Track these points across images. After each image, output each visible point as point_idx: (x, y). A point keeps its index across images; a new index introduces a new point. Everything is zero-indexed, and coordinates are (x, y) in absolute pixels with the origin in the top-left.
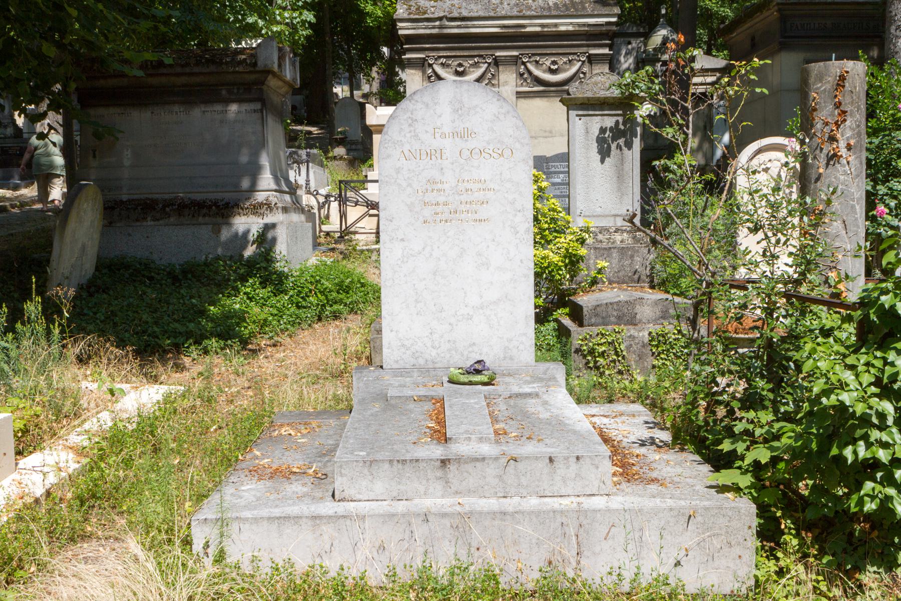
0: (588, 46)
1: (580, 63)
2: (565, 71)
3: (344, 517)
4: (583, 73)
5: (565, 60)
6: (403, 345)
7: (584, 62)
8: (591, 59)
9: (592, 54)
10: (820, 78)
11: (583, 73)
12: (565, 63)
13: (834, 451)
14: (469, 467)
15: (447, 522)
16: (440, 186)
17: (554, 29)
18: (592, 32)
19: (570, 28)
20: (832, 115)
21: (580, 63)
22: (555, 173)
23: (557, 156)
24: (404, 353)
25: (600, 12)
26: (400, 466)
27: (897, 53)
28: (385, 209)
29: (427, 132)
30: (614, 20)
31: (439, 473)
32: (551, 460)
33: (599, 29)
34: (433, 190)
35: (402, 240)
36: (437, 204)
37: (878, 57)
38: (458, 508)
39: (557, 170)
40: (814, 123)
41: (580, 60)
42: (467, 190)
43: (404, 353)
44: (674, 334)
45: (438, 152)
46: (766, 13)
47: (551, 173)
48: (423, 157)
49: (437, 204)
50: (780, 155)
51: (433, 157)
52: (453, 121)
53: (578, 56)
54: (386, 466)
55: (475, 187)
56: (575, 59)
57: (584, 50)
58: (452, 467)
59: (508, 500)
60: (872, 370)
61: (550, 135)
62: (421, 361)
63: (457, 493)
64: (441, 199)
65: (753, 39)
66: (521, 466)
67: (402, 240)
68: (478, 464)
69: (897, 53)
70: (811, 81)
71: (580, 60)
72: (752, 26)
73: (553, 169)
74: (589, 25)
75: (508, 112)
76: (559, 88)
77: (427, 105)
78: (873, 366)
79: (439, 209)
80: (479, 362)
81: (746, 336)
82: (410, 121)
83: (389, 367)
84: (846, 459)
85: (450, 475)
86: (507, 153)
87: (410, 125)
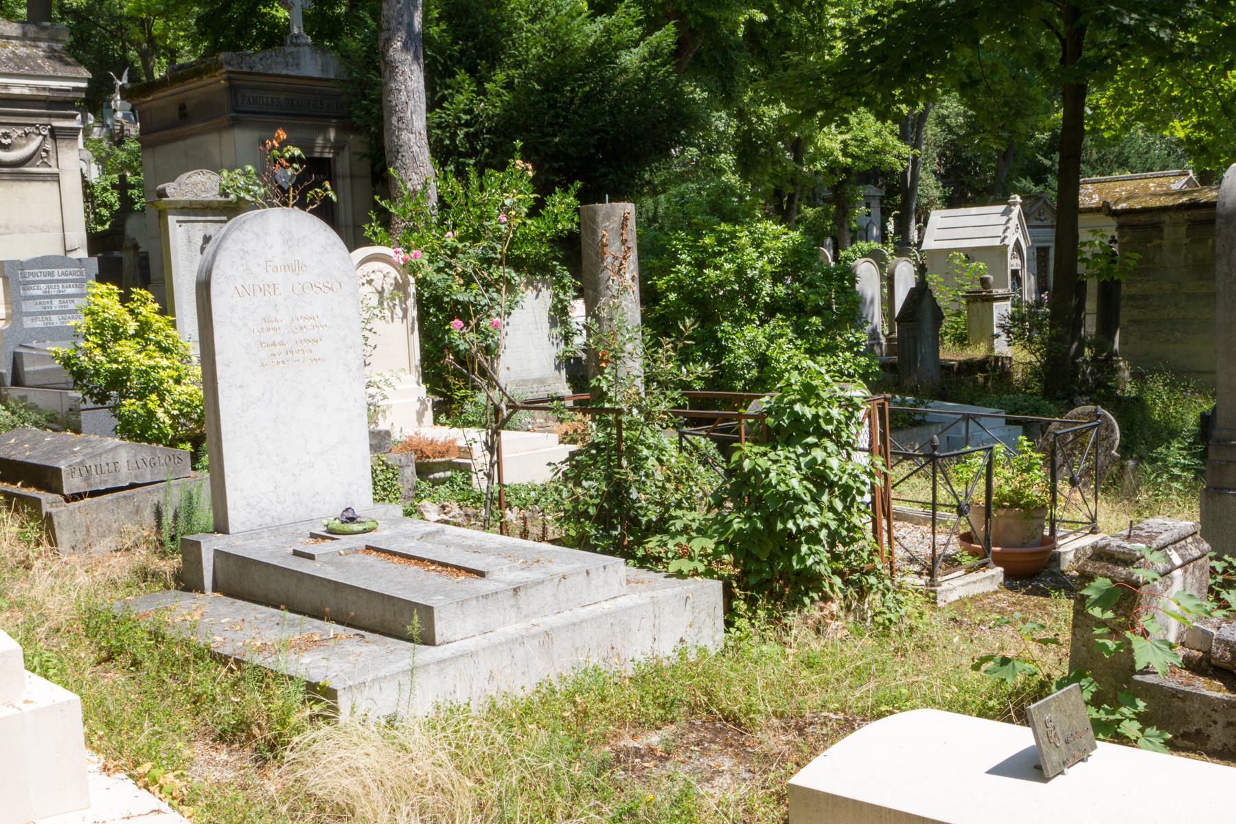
0: (50, 116)
1: (41, 137)
2: (21, 146)
3: (462, 656)
4: (45, 151)
5: (20, 132)
6: (249, 504)
7: (45, 136)
8: (54, 134)
9: (56, 128)
10: (608, 217)
11: (45, 151)
12: (20, 137)
13: (780, 526)
14: (533, 591)
15: (536, 642)
16: (275, 325)
17: (4, 91)
18: (56, 99)
19: (26, 91)
20: (620, 250)
21: (41, 137)
22: (34, 282)
23: (35, 260)
24: (251, 513)
25: (65, 74)
26: (484, 601)
27: (401, 146)
28: (221, 353)
29: (259, 265)
30: (84, 85)
31: (512, 602)
32: (588, 573)
33: (64, 95)
34: (268, 329)
35: (241, 386)
36: (274, 344)
37: (336, 139)
38: (534, 630)
39: (36, 278)
40: (605, 256)
41: (40, 134)
42: (301, 328)
43: (251, 513)
44: (379, 465)
45: (272, 287)
46: (206, 80)
47: (29, 283)
48: (257, 292)
49: (274, 344)
50: (386, 268)
51: (267, 293)
52: (284, 253)
53: (37, 128)
54: (474, 603)
55: (309, 323)
56: (33, 133)
57: (45, 120)
58: (521, 594)
59: (561, 615)
60: (791, 462)
61: (7, 231)
62: (268, 520)
63: (526, 616)
64: (277, 339)
65: (182, 107)
66: (568, 581)
67: (241, 386)
68: (540, 587)
69: (401, 146)
70: (599, 219)
71: (40, 134)
72: (182, 92)
73: (31, 278)
74: (51, 90)
75: (335, 243)
76: (15, 170)
77: (258, 235)
78: (790, 458)
79: (276, 350)
80: (347, 509)
81: (443, 460)
82: (241, 254)
83: (236, 531)
84: (791, 530)
85: (521, 602)
86: (336, 286)
87: (242, 258)
